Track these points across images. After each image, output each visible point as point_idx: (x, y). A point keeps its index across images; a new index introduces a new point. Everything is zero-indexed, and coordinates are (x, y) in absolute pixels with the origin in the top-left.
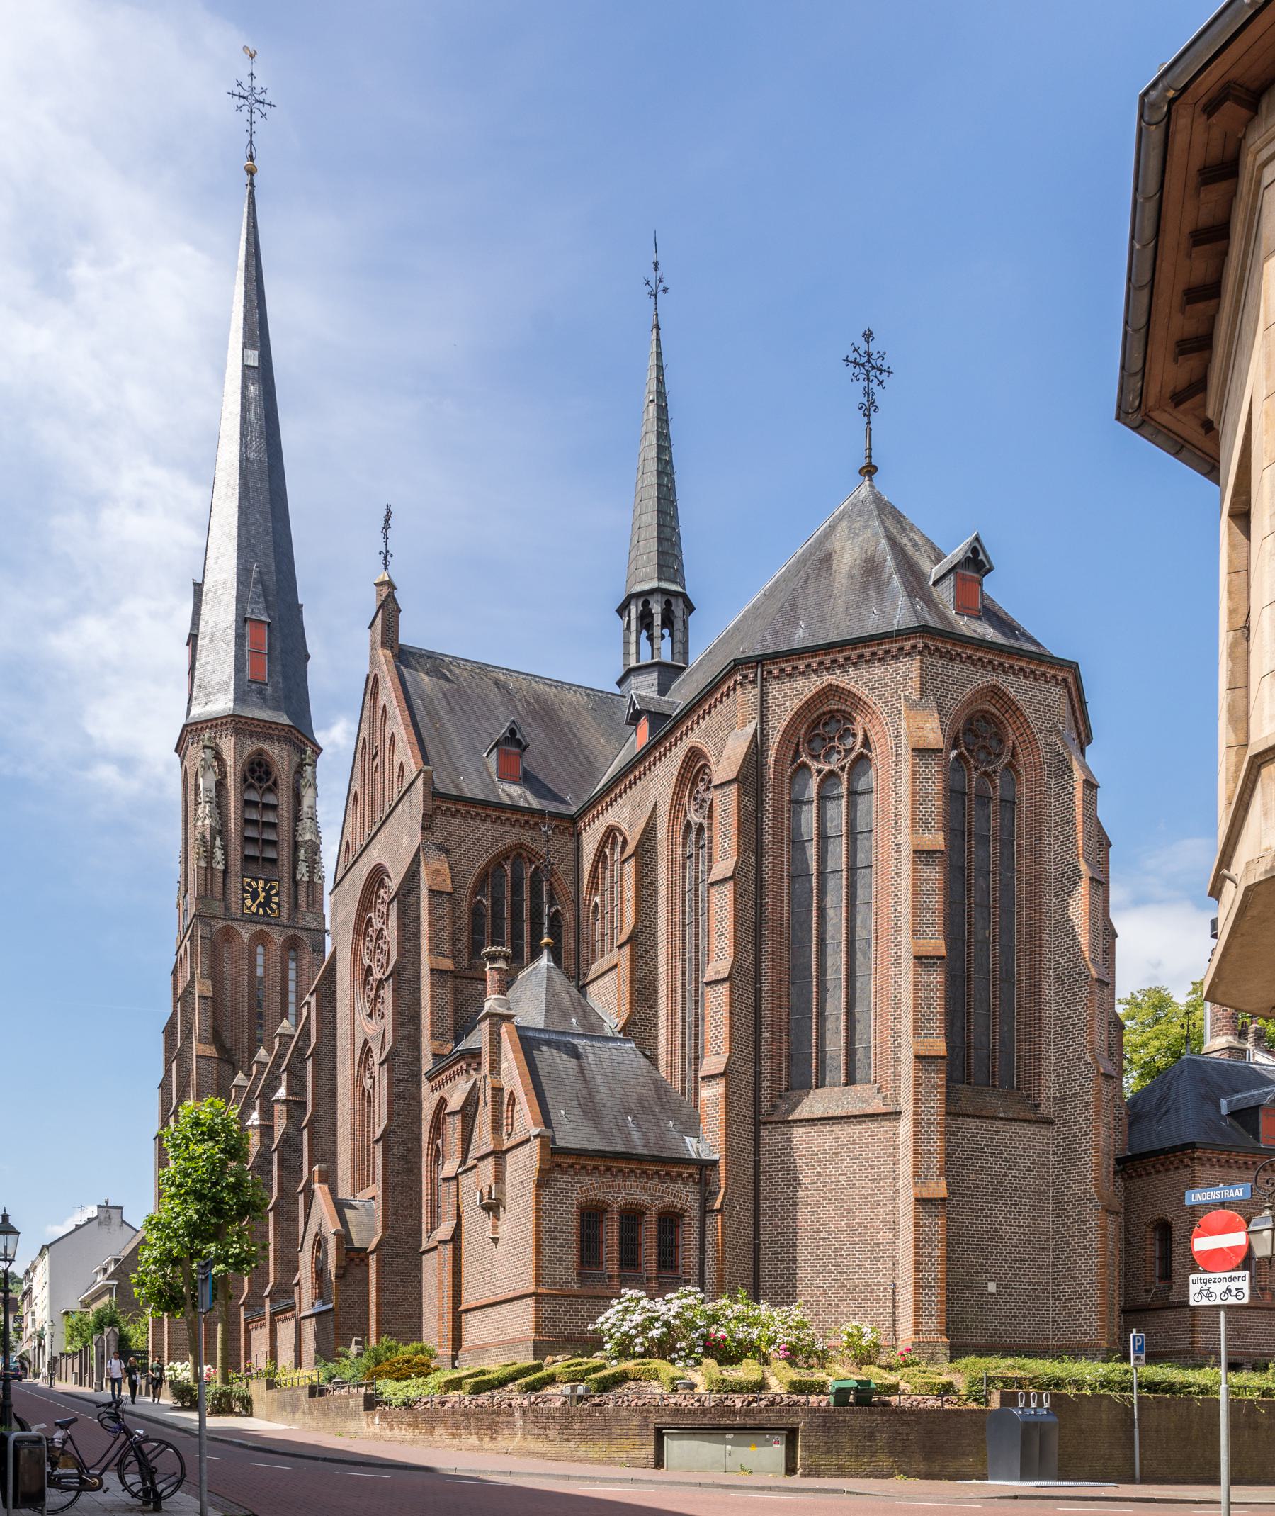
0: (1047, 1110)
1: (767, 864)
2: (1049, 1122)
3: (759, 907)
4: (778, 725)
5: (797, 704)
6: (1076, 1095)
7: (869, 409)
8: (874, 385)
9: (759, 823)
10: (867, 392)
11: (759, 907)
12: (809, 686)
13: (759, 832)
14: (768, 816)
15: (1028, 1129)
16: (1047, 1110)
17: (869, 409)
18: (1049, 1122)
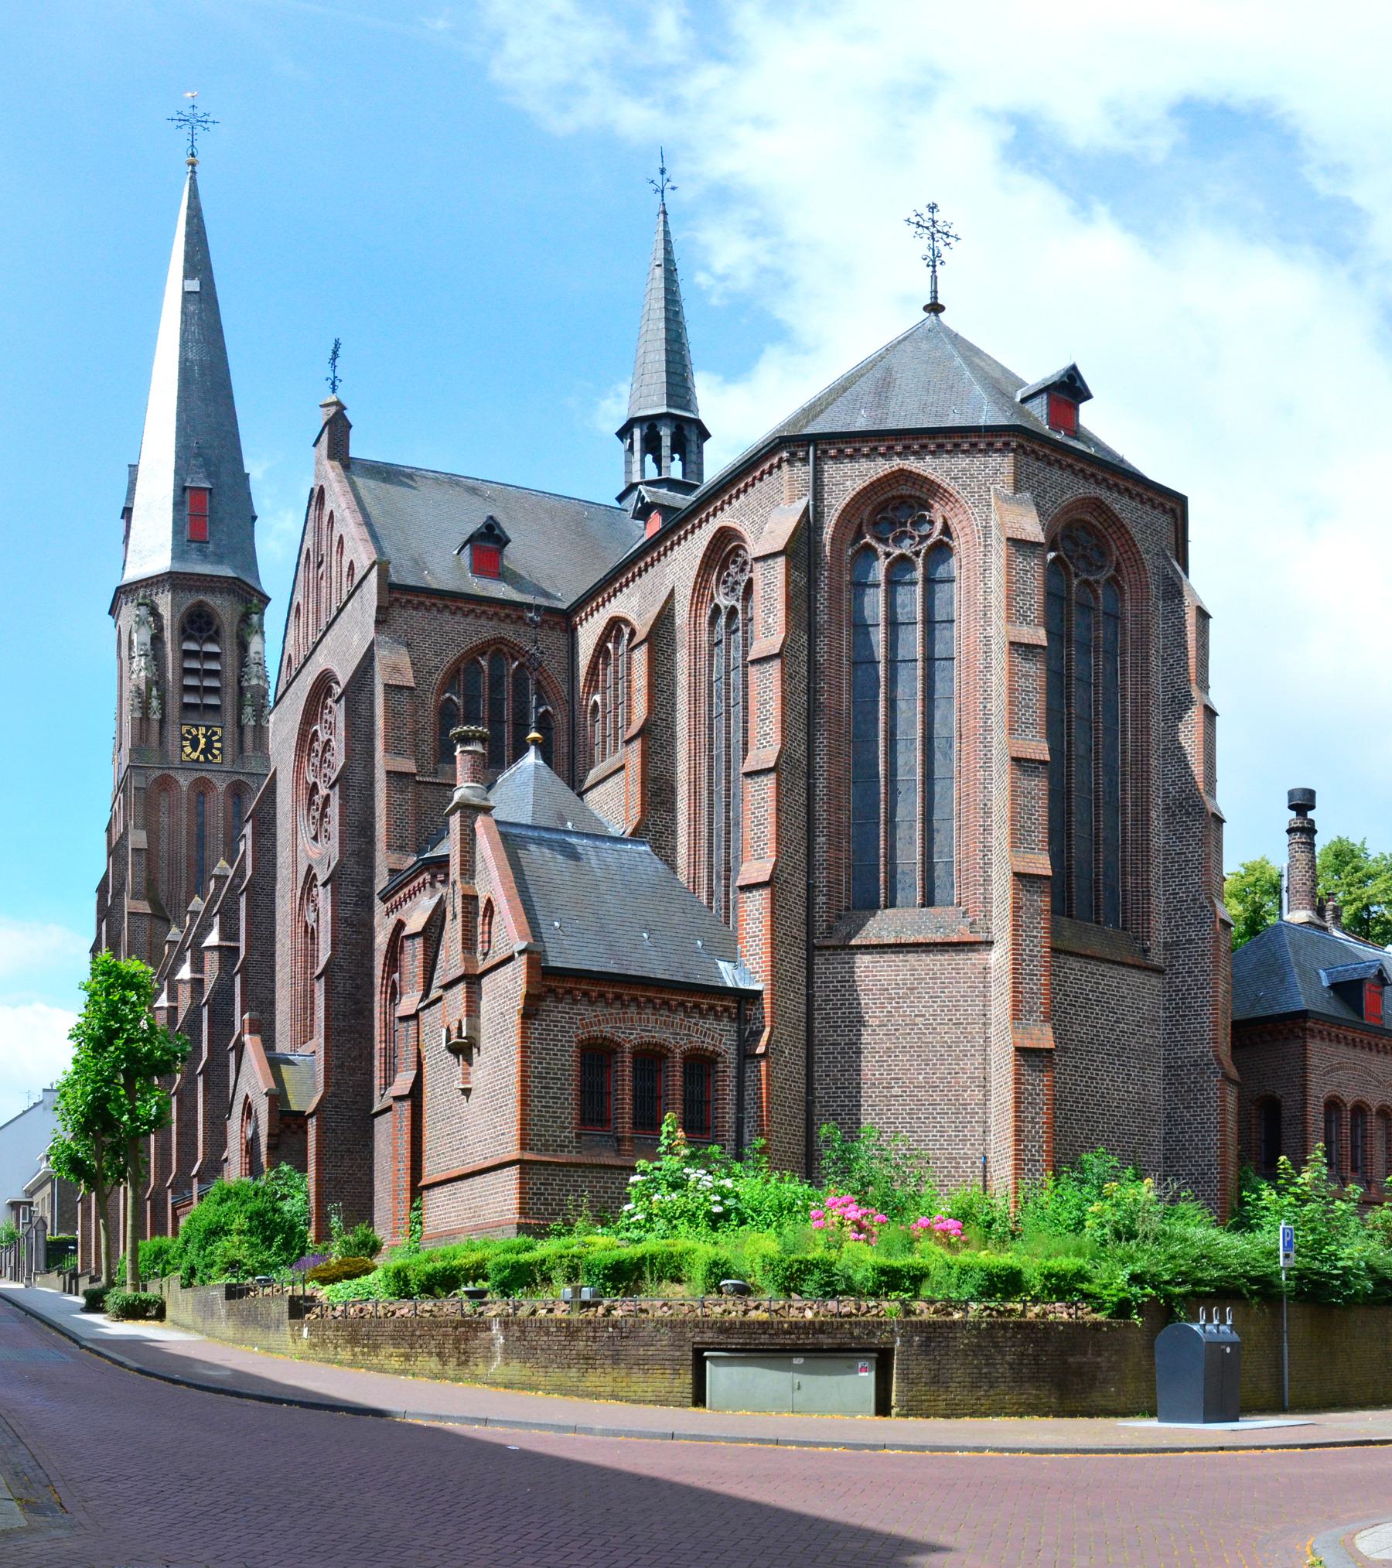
7: (934, 261)
8: (940, 245)
17: (934, 261)
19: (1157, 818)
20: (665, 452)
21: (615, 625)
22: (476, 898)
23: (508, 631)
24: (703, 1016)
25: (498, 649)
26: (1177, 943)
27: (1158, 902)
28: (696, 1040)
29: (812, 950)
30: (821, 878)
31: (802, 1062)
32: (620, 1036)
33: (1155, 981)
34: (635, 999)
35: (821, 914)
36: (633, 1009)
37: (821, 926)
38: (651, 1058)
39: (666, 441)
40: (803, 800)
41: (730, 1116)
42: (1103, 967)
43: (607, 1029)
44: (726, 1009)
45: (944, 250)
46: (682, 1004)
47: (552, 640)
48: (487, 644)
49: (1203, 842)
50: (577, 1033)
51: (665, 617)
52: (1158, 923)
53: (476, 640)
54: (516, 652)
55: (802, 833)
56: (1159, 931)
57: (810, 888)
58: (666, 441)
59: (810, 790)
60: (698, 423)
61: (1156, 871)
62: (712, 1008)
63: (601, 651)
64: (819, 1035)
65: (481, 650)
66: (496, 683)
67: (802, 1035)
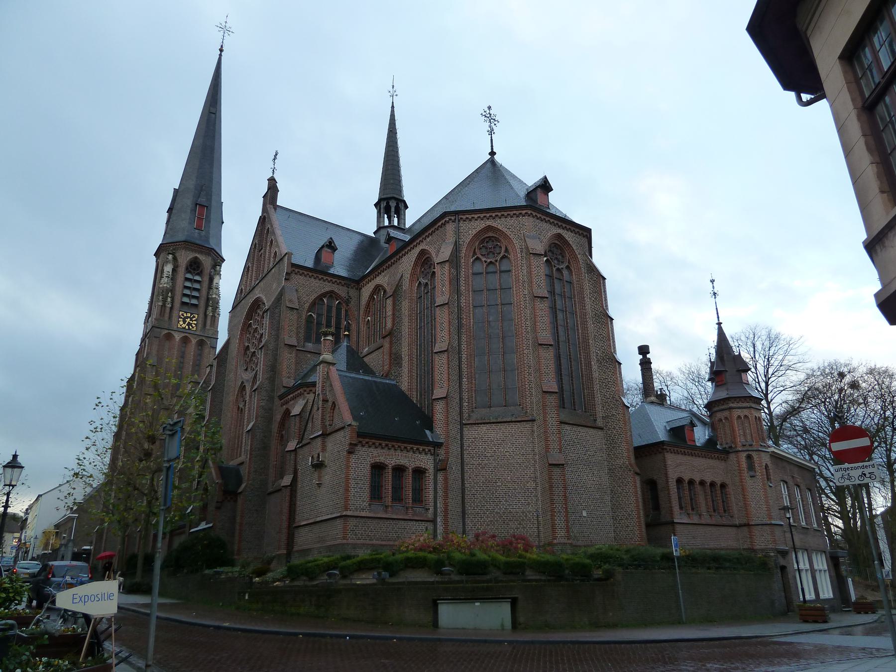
0: (600, 423)
1: (463, 300)
2: (601, 429)
3: (459, 319)
4: (466, 239)
5: (474, 232)
6: (613, 415)
7: (491, 132)
9: (458, 280)
10: (490, 127)
11: (459, 319)
12: (479, 225)
13: (458, 285)
14: (462, 279)
15: (592, 431)
16: (600, 423)
17: (491, 132)
18: (601, 429)
19: (595, 366)
20: (392, 213)
21: (378, 288)
22: (327, 401)
23: (336, 288)
24: (420, 453)
25: (331, 294)
26: (607, 416)
27: (598, 398)
28: (418, 464)
29: (462, 425)
30: (465, 396)
31: (460, 472)
32: (387, 462)
33: (600, 432)
34: (393, 446)
35: (465, 410)
36: (392, 450)
37: (466, 415)
38: (399, 470)
39: (393, 209)
40: (457, 363)
41: (431, 497)
42: (580, 428)
43: (382, 459)
44: (429, 450)
45: (494, 127)
46: (412, 448)
47: (353, 293)
48: (327, 293)
49: (614, 373)
50: (370, 460)
51: (399, 286)
52: (599, 408)
53: (323, 291)
54: (338, 297)
55: (457, 377)
56: (600, 412)
57: (461, 399)
58: (393, 209)
59: (460, 359)
60: (404, 202)
61: (596, 387)
62: (424, 450)
63: (371, 297)
64: (466, 461)
65: (324, 295)
66: (329, 308)
67: (460, 461)
